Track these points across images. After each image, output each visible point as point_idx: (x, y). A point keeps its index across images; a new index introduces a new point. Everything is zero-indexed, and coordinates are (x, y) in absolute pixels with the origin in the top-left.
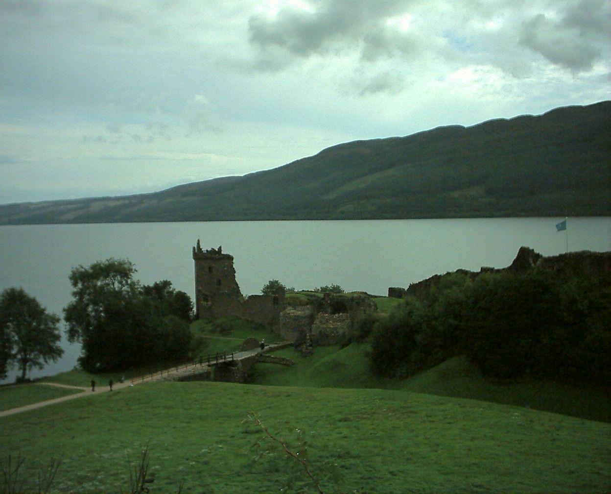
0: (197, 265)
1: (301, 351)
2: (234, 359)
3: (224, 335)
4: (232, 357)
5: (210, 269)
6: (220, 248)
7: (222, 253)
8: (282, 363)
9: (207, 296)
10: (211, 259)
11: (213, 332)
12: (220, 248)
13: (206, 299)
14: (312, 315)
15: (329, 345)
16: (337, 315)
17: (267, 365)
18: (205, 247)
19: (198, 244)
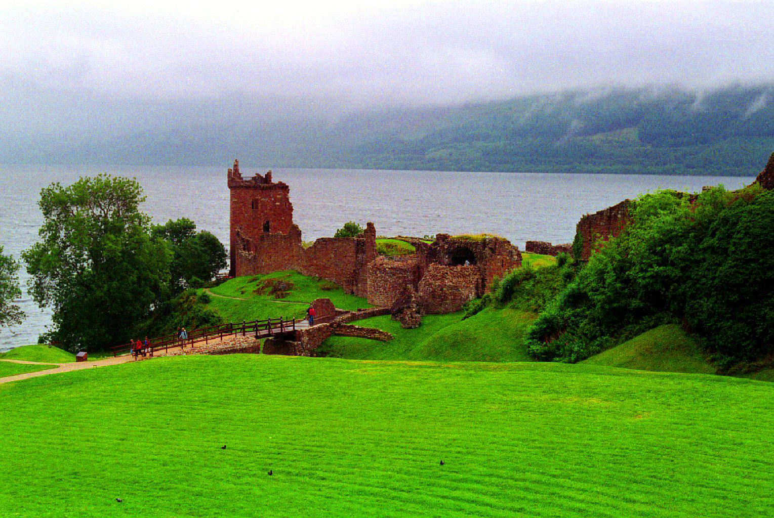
0: (232, 196)
2: (296, 328)
3: (278, 297)
4: (294, 326)
5: (255, 204)
6: (269, 175)
7: (273, 181)
8: (372, 336)
9: (248, 241)
10: (255, 188)
11: (259, 292)
12: (269, 175)
13: (247, 247)
14: (418, 267)
15: (446, 313)
16: (459, 267)
17: (347, 339)
18: (247, 174)
19: (236, 166)
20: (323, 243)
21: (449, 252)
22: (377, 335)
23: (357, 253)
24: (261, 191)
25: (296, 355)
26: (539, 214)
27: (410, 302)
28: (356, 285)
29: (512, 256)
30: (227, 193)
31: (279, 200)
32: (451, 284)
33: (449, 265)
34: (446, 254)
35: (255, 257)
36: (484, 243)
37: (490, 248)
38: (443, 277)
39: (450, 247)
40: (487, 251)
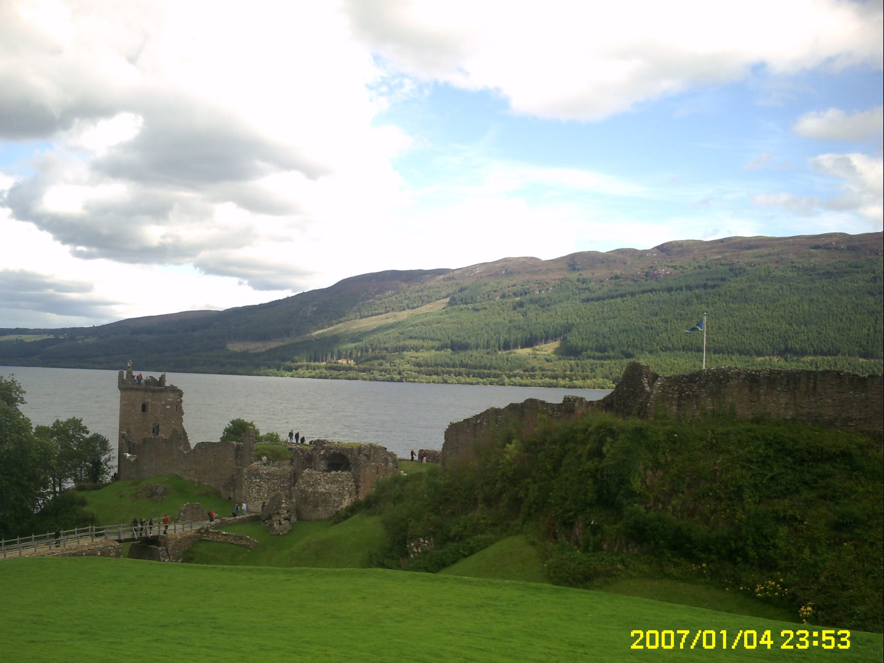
1: (271, 525)
5: (144, 408)
10: (146, 390)
12: (162, 379)
16: (333, 473)
20: (203, 446)
21: (324, 457)
22: (244, 542)
23: (236, 457)
24: (151, 394)
25: (160, 560)
26: (409, 420)
27: (280, 508)
28: (234, 490)
29: (387, 464)
30: (118, 393)
31: (171, 404)
32: (323, 490)
33: (326, 471)
34: (322, 459)
35: (137, 460)
36: (360, 449)
37: (365, 455)
38: (317, 483)
39: (327, 451)
40: (362, 458)
